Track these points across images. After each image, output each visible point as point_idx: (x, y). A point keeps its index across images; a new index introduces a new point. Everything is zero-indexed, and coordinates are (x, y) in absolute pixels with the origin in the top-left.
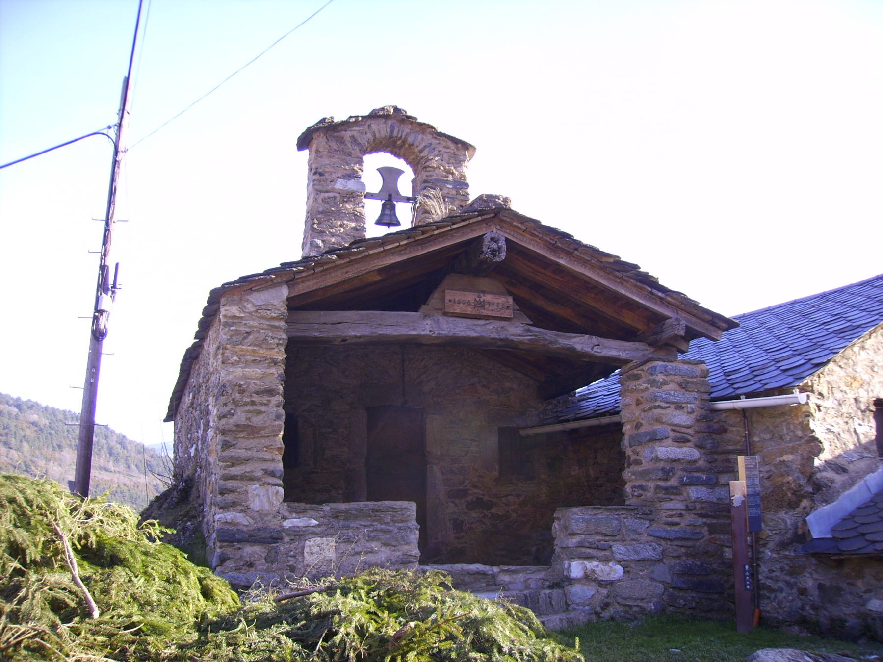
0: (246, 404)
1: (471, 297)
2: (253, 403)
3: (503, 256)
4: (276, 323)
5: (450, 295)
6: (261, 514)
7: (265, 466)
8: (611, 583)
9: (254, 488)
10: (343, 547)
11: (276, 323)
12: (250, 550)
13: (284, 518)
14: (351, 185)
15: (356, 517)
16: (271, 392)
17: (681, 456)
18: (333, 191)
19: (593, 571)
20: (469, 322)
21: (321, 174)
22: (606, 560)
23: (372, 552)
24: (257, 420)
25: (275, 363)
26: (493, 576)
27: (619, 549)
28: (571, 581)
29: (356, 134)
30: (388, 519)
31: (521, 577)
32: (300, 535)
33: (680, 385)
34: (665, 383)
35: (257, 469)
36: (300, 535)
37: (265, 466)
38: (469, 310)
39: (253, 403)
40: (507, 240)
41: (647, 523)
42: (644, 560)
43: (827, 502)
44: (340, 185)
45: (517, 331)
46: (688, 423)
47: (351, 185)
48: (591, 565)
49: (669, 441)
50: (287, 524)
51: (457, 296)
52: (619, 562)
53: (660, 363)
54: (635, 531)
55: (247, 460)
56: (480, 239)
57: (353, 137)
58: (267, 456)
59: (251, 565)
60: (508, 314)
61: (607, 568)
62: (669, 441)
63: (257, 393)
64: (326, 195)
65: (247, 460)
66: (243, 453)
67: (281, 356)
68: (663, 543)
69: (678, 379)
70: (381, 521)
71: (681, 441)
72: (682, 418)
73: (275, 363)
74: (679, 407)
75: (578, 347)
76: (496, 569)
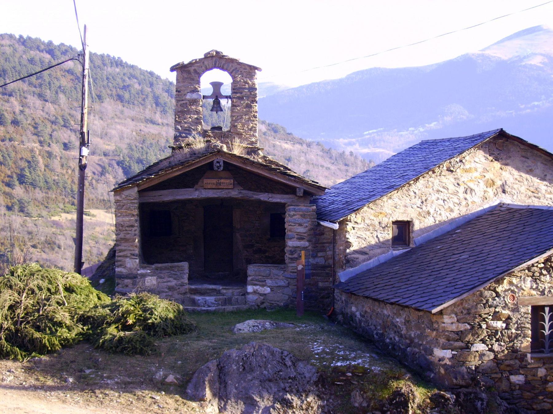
0: (124, 231)
1: (215, 181)
2: (126, 230)
3: (222, 168)
4: (133, 201)
5: (206, 181)
6: (130, 269)
7: (131, 252)
8: (265, 294)
9: (128, 260)
10: (159, 280)
11: (133, 201)
12: (127, 281)
13: (138, 270)
14: (194, 96)
15: (164, 269)
16: (132, 226)
17: (299, 245)
18: (186, 100)
19: (257, 290)
20: (215, 191)
21: (179, 92)
22: (263, 286)
23: (169, 281)
24: (128, 236)
25: (133, 215)
26: (219, 290)
27: (269, 282)
28: (248, 293)
29: (196, 68)
30: (176, 270)
31: (231, 291)
32: (143, 276)
33: (301, 215)
34: (294, 215)
35: (128, 253)
36: (143, 276)
37: (131, 252)
38: (214, 187)
39: (126, 230)
40: (224, 162)
41: (282, 272)
42: (280, 286)
43: (352, 267)
44: (189, 96)
45: (235, 193)
46: (304, 231)
47: (194, 96)
48: (256, 288)
49: (295, 239)
50: (139, 272)
51: (209, 182)
52: (269, 287)
53: (292, 207)
54: (277, 275)
55: (125, 250)
56: (212, 162)
57: (195, 70)
58: (132, 249)
59: (127, 286)
60: (231, 187)
61: (263, 289)
62: (295, 239)
63: (127, 227)
64: (182, 102)
65: (125, 250)
66: (123, 248)
67: (136, 212)
68: (289, 280)
69: (301, 213)
70: (173, 271)
71: (301, 239)
72: (301, 230)
73: (133, 215)
74: (300, 225)
75: (262, 199)
76: (221, 288)
